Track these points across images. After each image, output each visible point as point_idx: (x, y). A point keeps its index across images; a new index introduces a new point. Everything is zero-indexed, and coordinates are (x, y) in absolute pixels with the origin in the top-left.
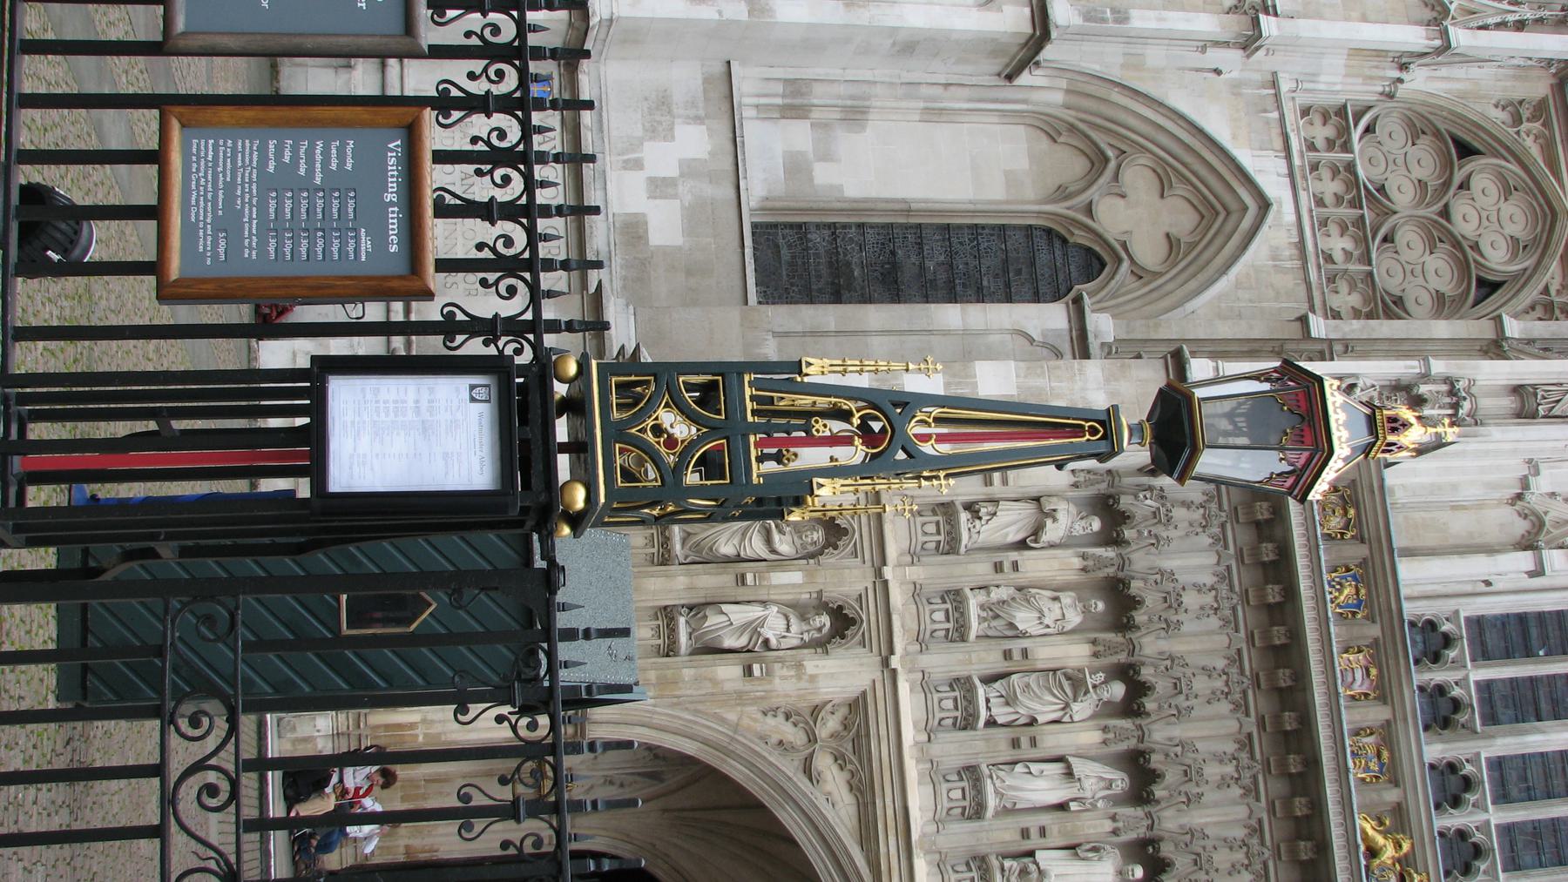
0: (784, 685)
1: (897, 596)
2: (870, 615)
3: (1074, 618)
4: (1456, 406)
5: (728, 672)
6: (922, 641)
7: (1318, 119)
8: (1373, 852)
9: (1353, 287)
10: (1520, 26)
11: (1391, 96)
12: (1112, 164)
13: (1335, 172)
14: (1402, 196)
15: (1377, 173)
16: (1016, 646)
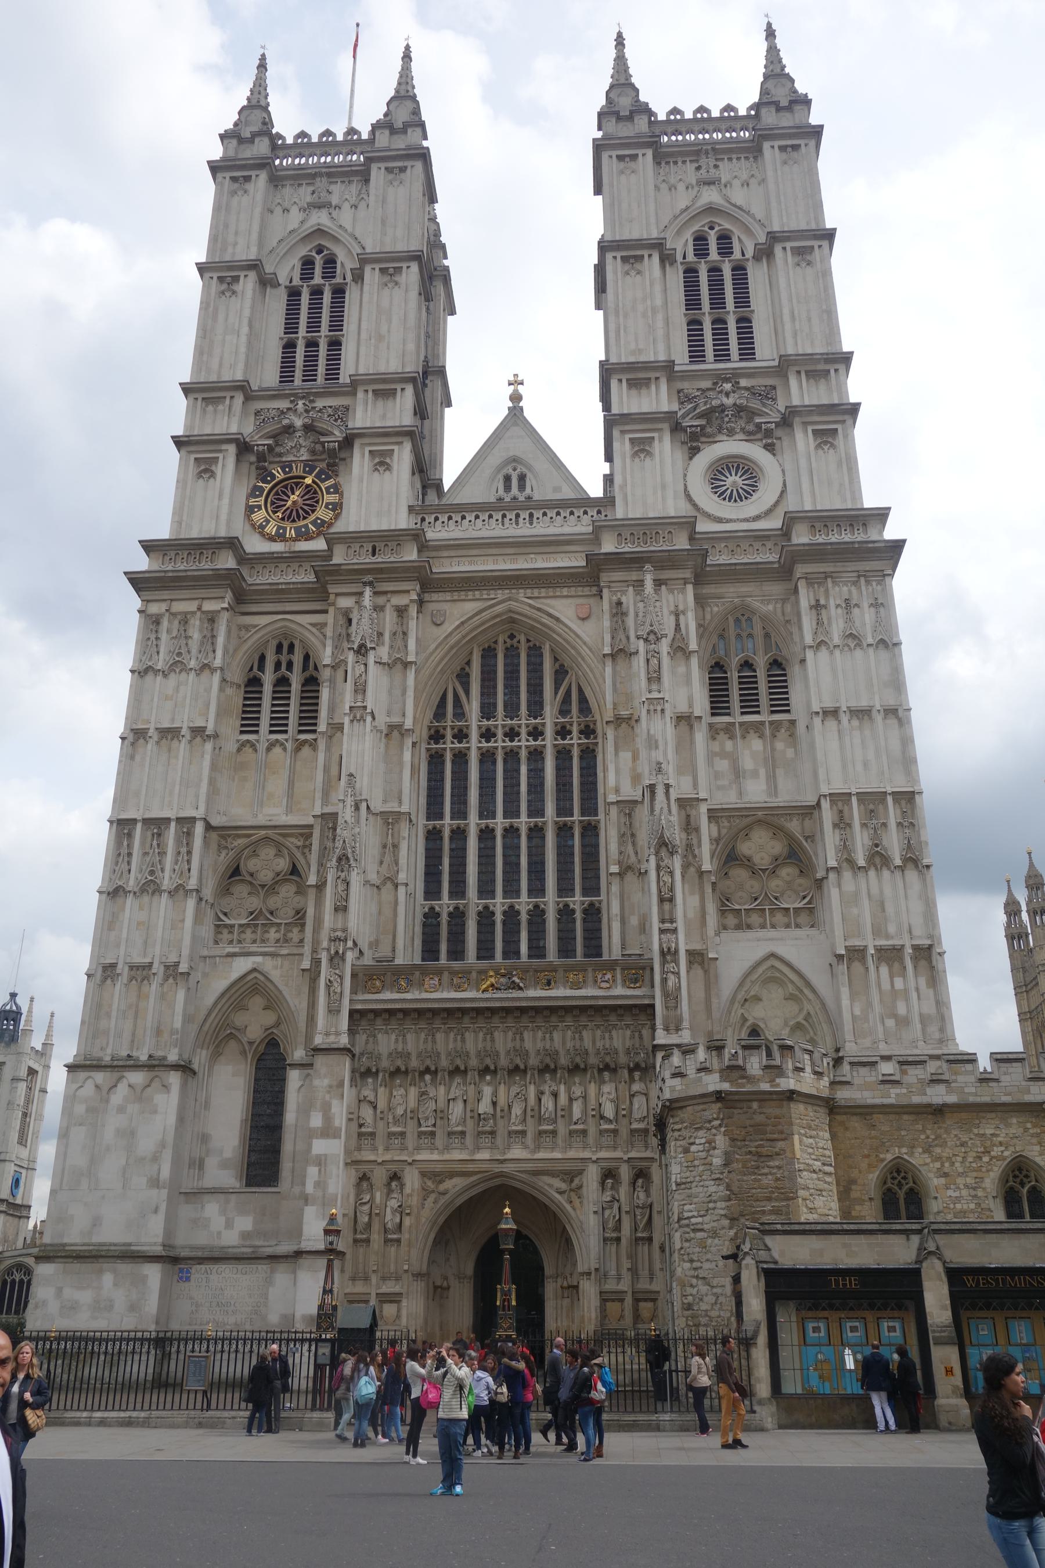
0: (414, 1201)
1: (388, 1157)
2: (393, 1167)
3: (402, 1091)
4: (340, 940)
5: (407, 1221)
6: (403, 1148)
7: (220, 936)
8: (492, 985)
9: (291, 931)
10: (189, 853)
11: (212, 905)
12: (233, 1031)
13: (243, 932)
14: (255, 903)
15: (246, 914)
16: (409, 1115)
